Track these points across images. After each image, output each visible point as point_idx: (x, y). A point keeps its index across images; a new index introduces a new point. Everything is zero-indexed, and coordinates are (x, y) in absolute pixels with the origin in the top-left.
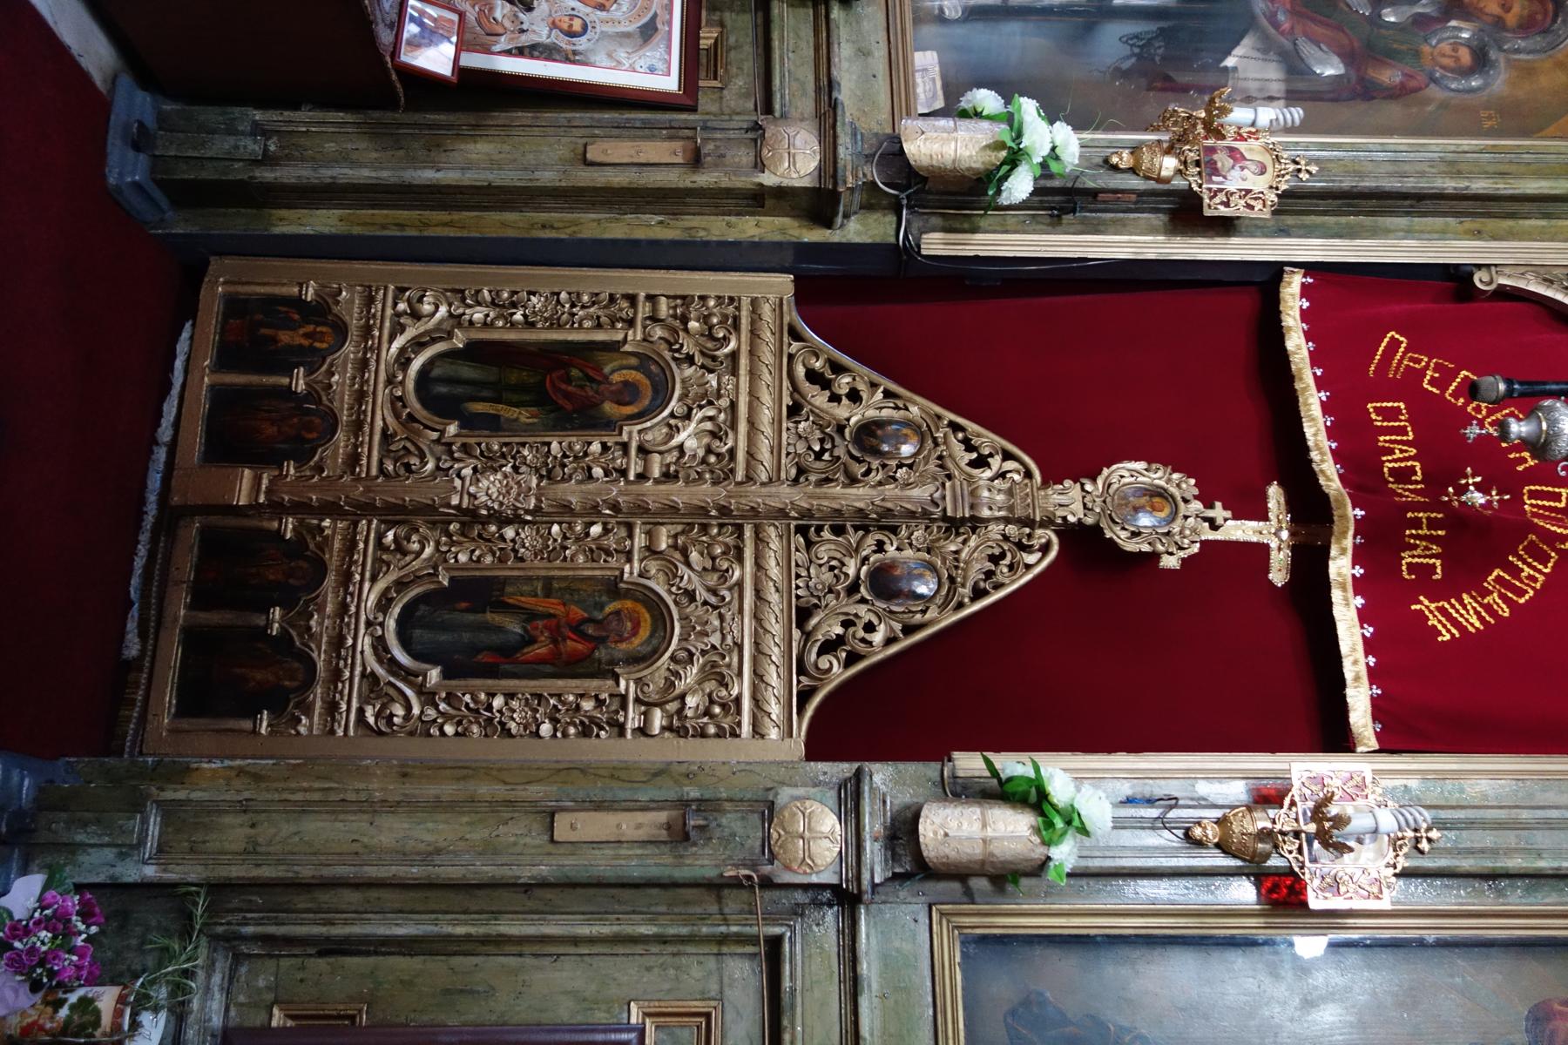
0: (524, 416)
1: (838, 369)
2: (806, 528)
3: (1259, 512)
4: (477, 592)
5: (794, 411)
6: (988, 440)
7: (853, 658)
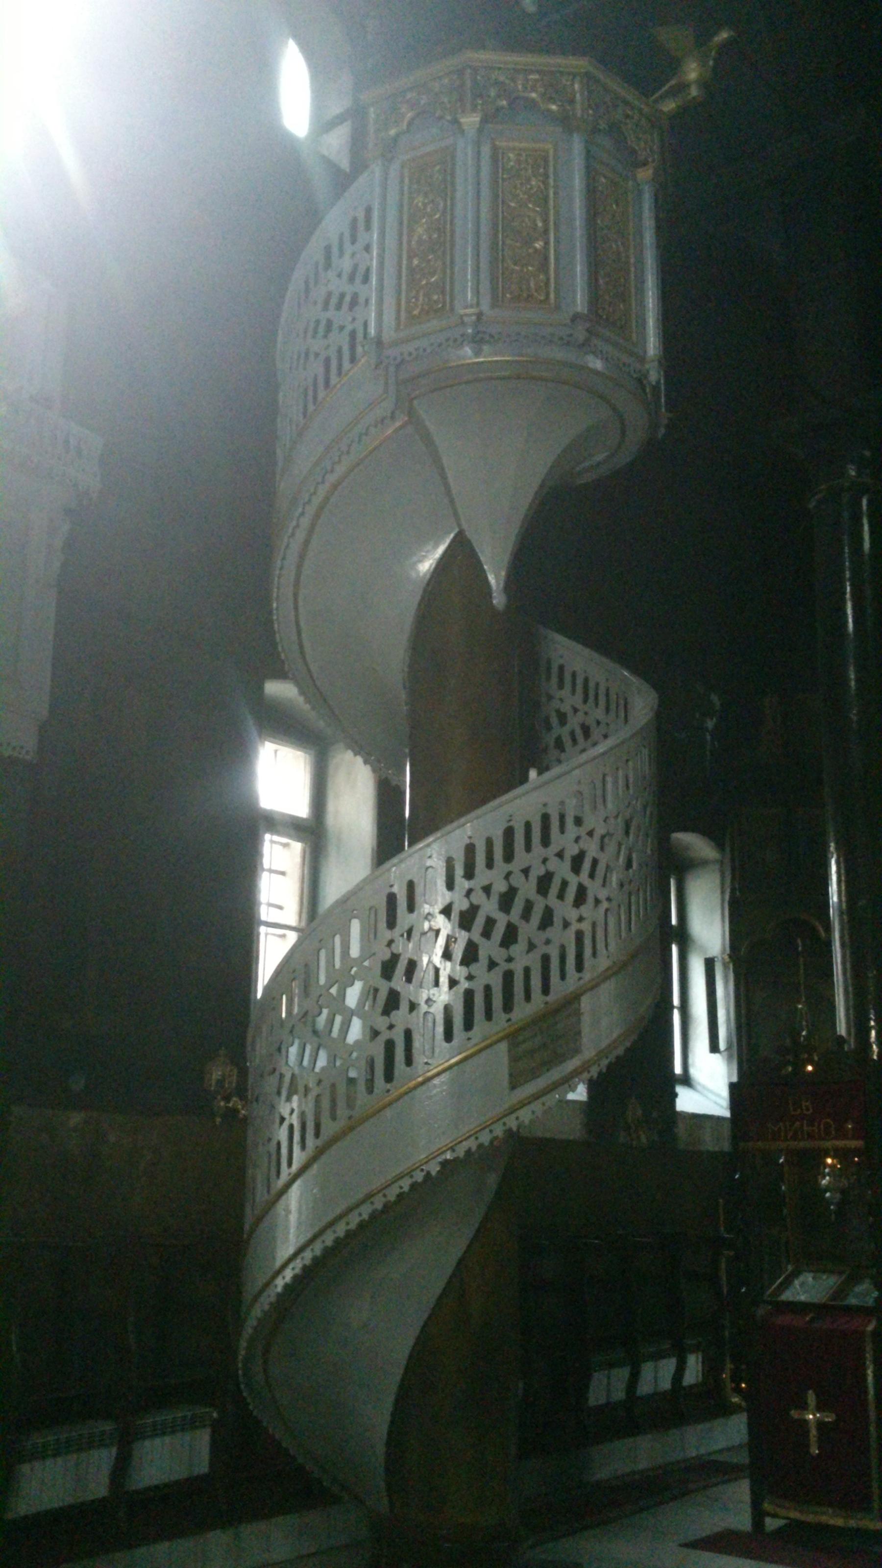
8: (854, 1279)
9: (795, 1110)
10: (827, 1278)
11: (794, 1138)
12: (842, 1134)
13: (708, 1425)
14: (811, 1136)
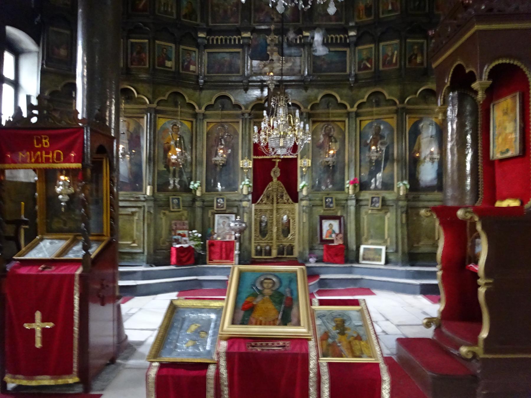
2: (278, 203)
3: (275, 162)
4: (283, 231)
5: (265, 204)
11: (37, 162)
12: (67, 160)
14: (47, 160)
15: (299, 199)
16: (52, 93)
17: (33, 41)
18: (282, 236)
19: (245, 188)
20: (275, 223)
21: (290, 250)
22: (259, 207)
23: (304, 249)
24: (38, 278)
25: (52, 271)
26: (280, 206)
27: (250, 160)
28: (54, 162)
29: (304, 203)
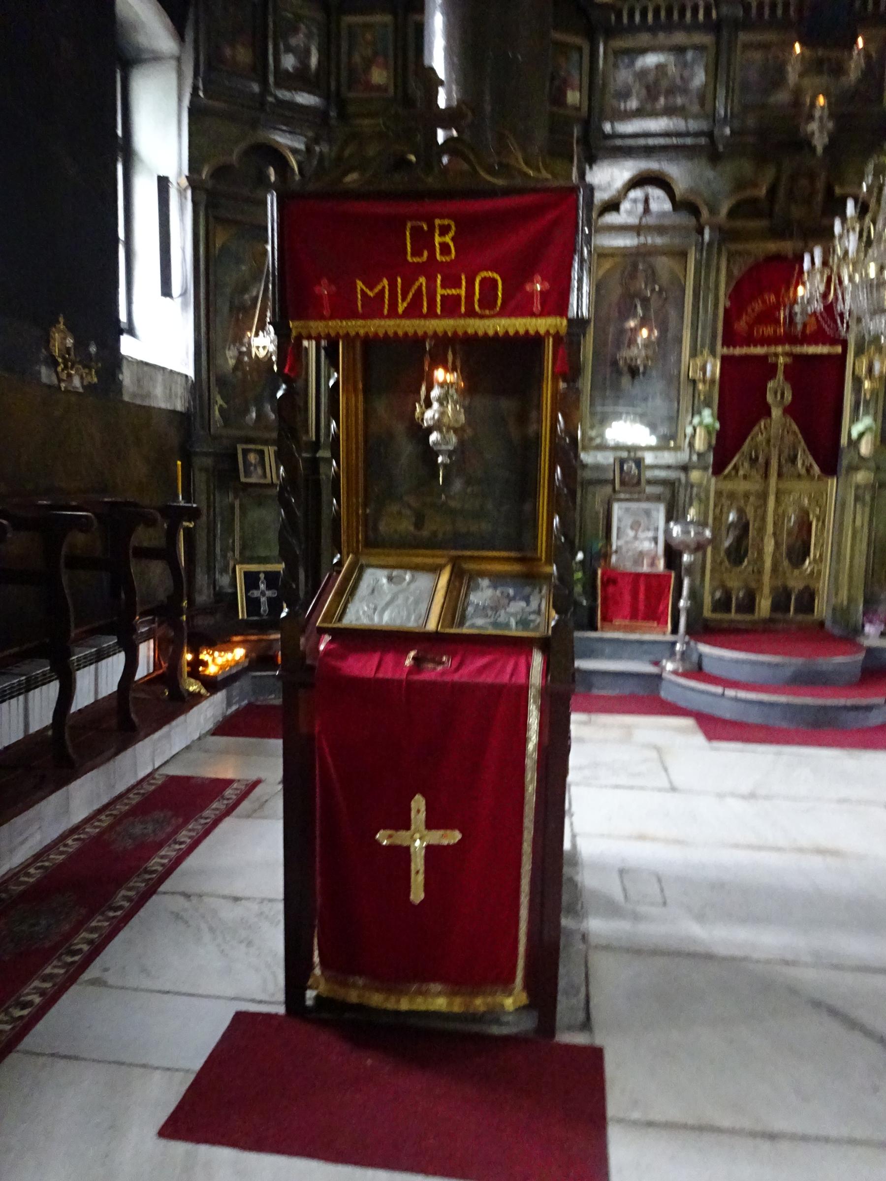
0: (744, 543)
1: (735, 465)
2: (780, 475)
5: (745, 477)
6: (756, 429)
7: (811, 466)
8: (462, 581)
9: (416, 253)
10: (413, 580)
11: (413, 311)
13: (165, 729)
14: (451, 307)
15: (844, 462)
16: (220, 172)
17: (168, 20)
18: (786, 563)
19: (700, 434)
20: (770, 528)
21: (807, 600)
22: (729, 486)
23: (851, 599)
24: (413, 690)
25: (442, 669)
26: (787, 485)
27: (714, 356)
28: (471, 313)
29: (861, 477)
